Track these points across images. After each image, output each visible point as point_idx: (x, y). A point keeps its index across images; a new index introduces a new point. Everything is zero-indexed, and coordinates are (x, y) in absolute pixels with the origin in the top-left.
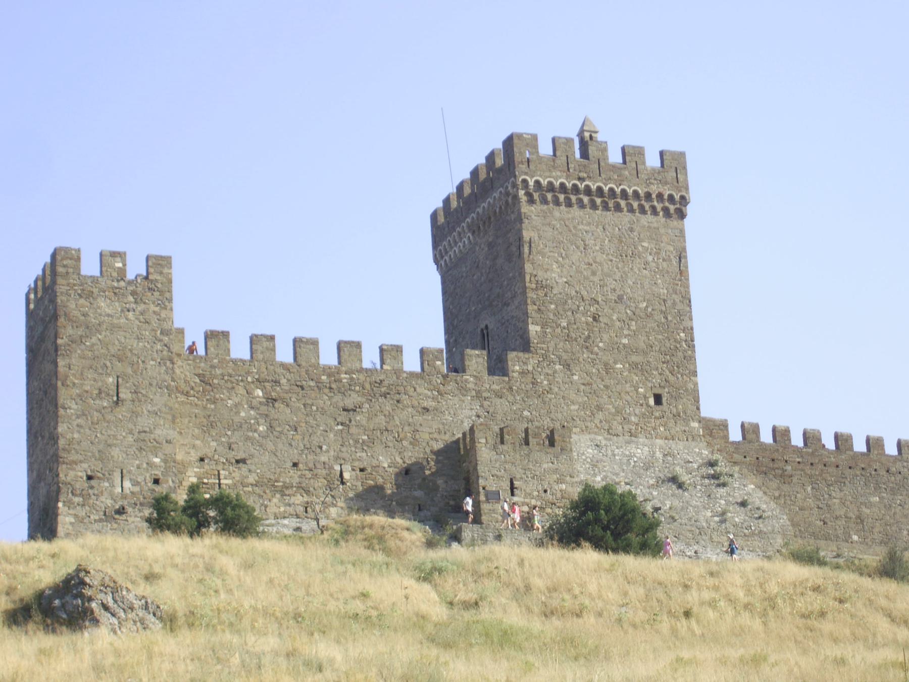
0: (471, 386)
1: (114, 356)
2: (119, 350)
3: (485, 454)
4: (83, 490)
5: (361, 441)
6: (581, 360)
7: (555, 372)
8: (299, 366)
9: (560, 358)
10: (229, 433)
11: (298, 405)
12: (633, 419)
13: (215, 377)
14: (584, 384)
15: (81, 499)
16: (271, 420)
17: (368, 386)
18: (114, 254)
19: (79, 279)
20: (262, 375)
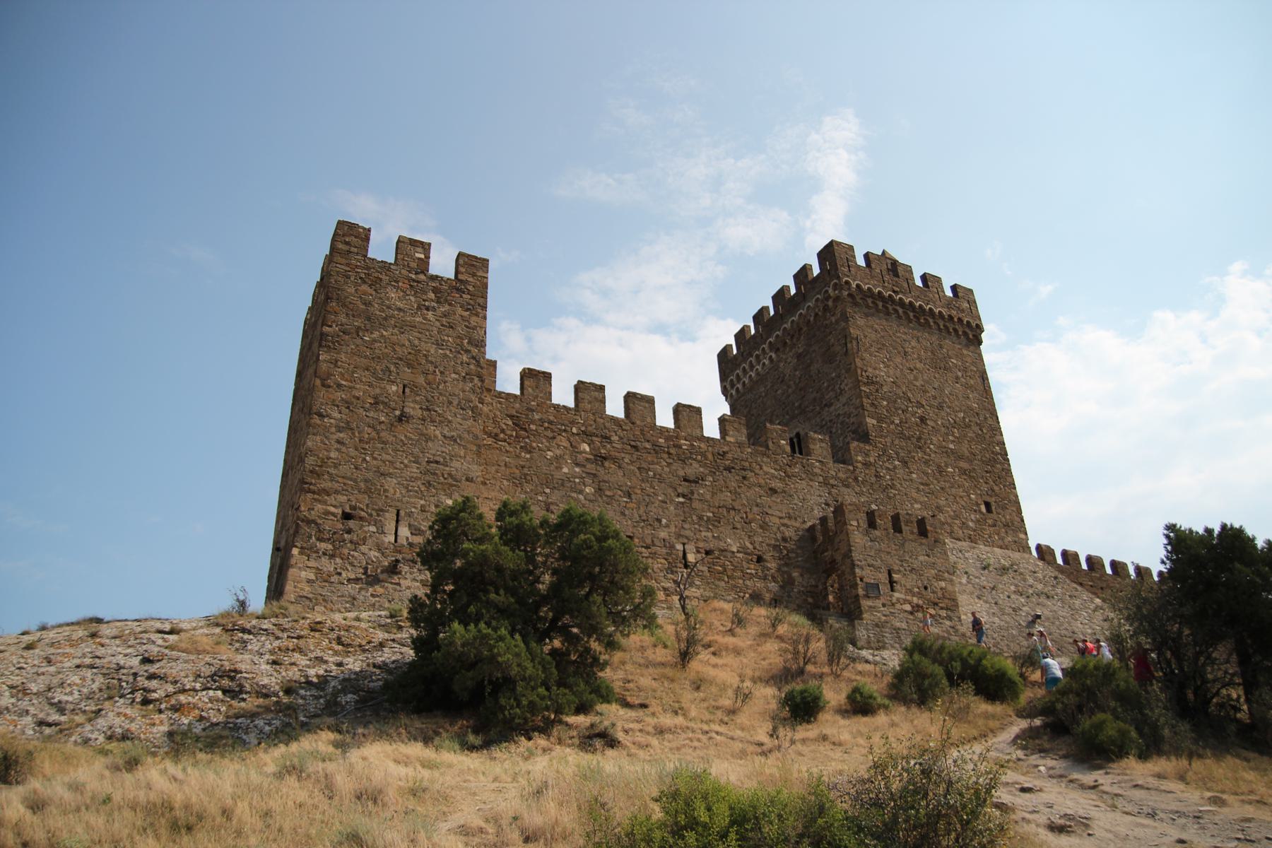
1: (401, 359)
2: (410, 353)
3: (858, 538)
4: (335, 533)
5: (705, 518)
6: (916, 459)
7: (895, 467)
8: (633, 423)
9: (897, 453)
10: (548, 491)
11: (632, 468)
12: (971, 524)
13: (533, 422)
14: (922, 484)
15: (330, 547)
16: (600, 482)
17: (710, 457)
18: (414, 243)
19: (364, 260)
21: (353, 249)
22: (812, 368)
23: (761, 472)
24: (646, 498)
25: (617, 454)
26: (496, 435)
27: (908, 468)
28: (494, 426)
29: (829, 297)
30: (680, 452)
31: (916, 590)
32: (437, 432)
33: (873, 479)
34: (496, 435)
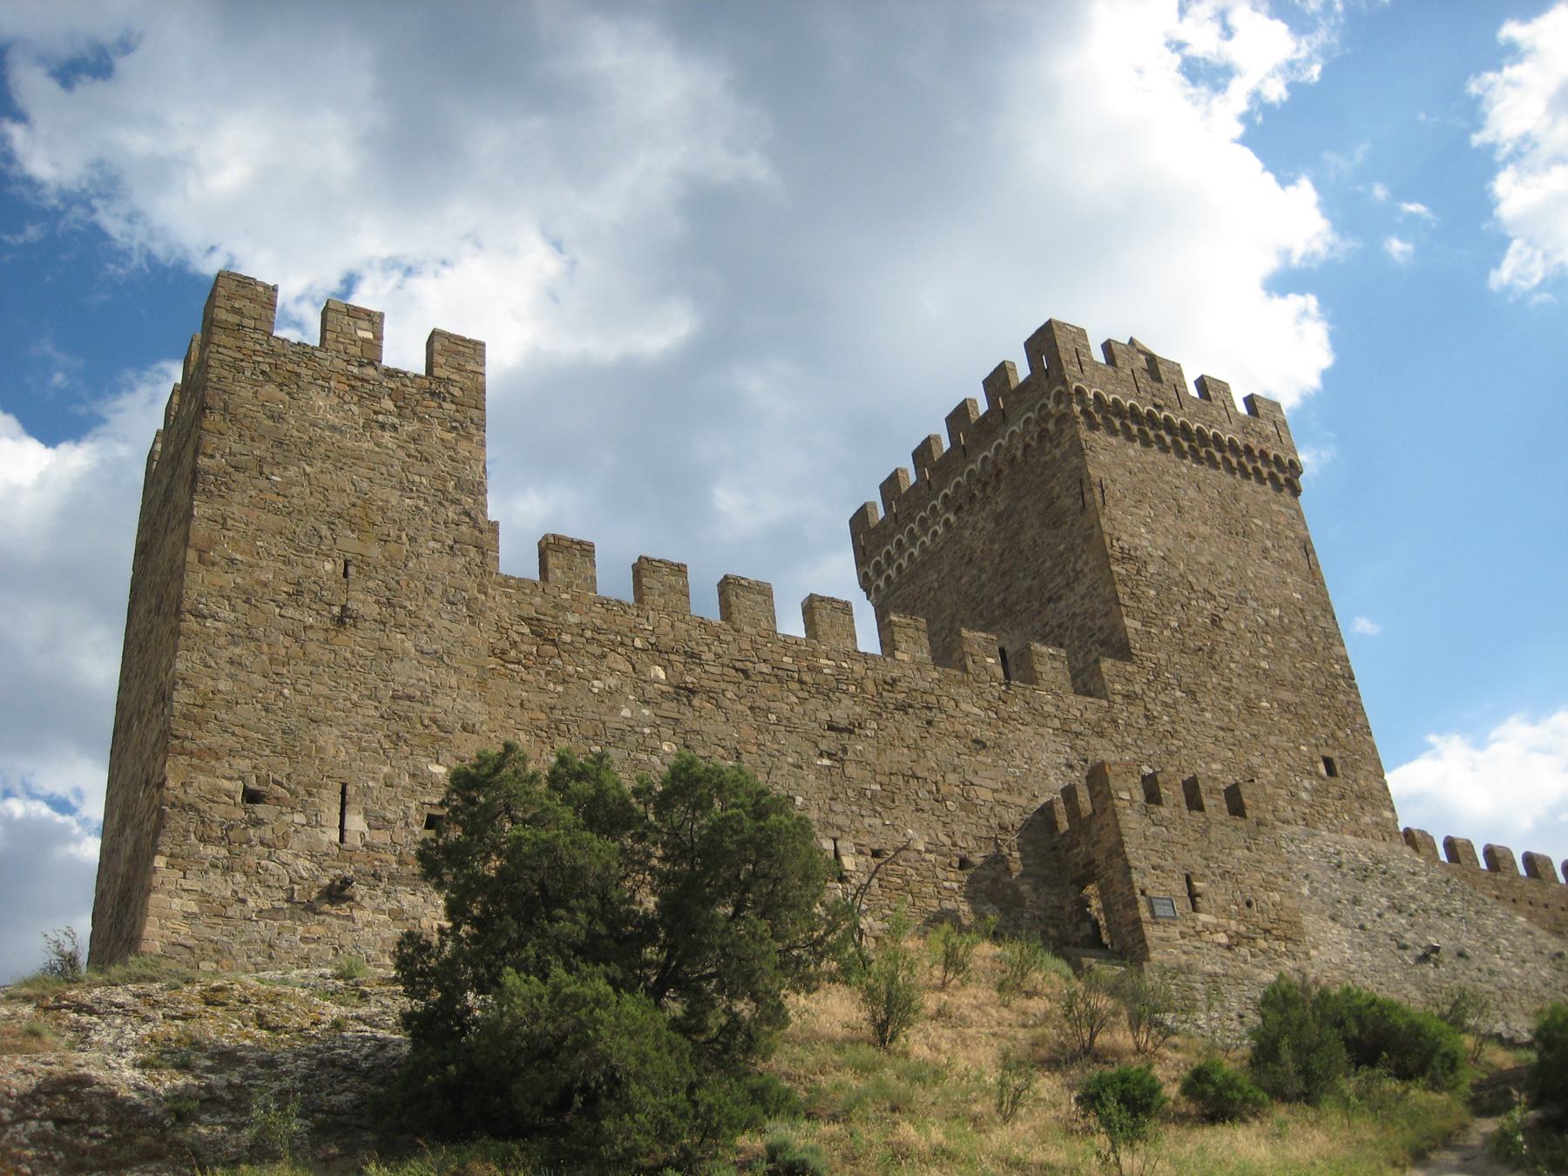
0: (1049, 709)
1: (340, 516)
2: (354, 505)
3: (1132, 822)
4: (231, 827)
5: (868, 793)
6: (1209, 686)
7: (1176, 702)
11: (740, 707)
12: (1304, 795)
13: (562, 629)
14: (1222, 729)
15: (224, 852)
17: (870, 686)
19: (268, 341)
20: (664, 639)
21: (246, 322)
22: (1022, 537)
23: (957, 713)
24: (766, 759)
25: (714, 684)
26: (504, 652)
27: (1198, 703)
28: (499, 636)
29: (1049, 415)
30: (820, 679)
31: (1234, 907)
32: (408, 644)
33: (1143, 722)
34: (504, 652)
